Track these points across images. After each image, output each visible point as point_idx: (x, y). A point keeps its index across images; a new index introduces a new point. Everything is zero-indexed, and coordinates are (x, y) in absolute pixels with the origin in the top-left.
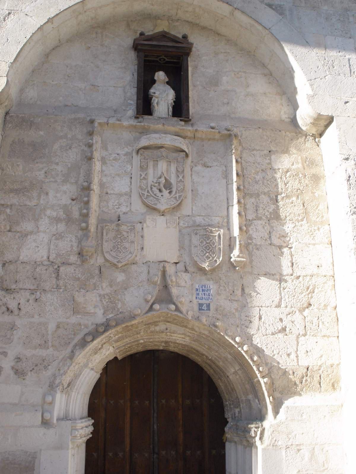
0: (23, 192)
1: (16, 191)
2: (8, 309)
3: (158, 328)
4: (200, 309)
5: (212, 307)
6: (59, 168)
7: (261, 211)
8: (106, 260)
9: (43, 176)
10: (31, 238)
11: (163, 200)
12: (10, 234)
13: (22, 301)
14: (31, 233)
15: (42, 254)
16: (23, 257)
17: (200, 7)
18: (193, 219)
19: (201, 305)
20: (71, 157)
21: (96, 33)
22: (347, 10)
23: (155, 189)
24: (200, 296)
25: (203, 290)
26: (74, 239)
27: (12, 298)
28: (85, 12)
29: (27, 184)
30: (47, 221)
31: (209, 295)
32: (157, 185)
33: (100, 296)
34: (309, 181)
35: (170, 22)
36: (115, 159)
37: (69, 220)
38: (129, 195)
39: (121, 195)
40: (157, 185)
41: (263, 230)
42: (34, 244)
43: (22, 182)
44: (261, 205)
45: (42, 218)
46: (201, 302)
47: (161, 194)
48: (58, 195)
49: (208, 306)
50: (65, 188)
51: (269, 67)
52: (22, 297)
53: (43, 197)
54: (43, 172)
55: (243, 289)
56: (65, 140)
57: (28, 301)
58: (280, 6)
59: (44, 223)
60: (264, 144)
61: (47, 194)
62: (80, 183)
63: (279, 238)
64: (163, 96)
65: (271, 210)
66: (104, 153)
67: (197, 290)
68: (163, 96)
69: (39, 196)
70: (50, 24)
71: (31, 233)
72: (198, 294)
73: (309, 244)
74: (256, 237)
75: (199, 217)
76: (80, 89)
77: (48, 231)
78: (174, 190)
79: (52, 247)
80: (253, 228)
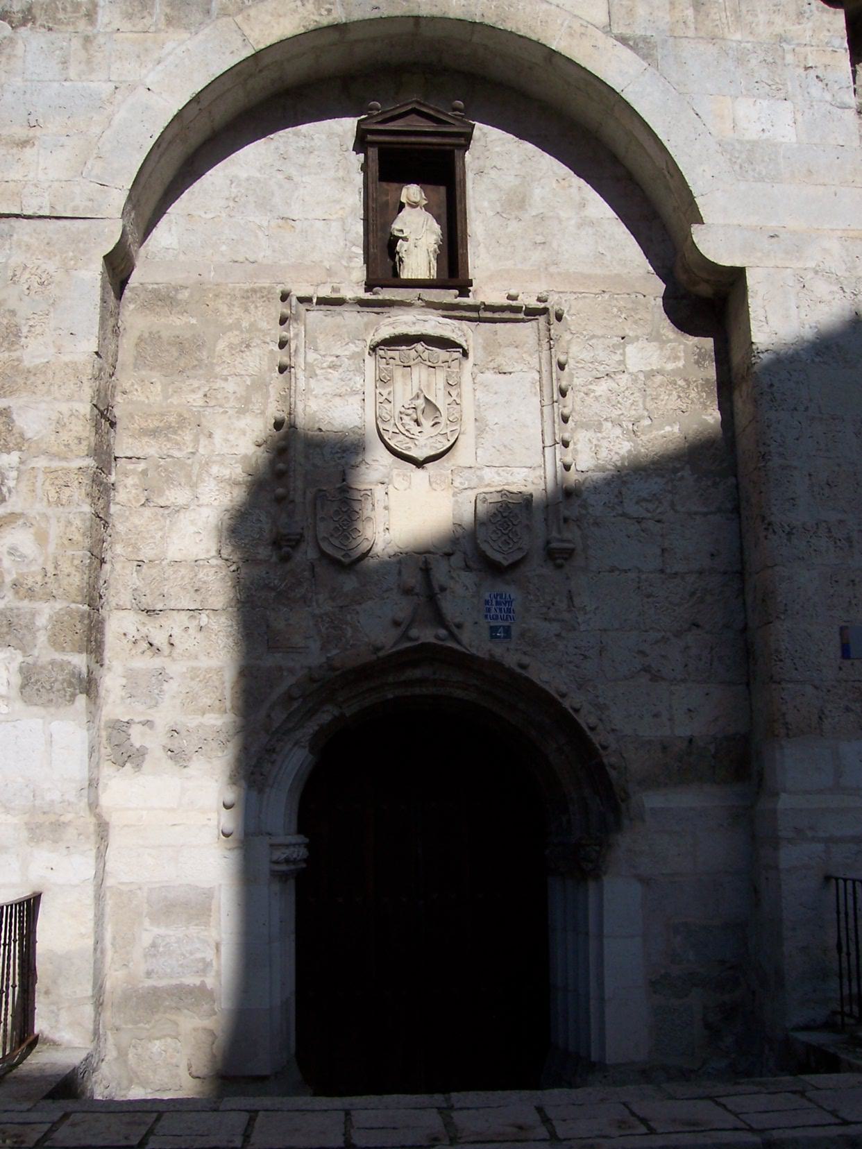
0: (166, 435)
1: (153, 433)
4: (492, 637)
5: (515, 632)
6: (231, 386)
8: (323, 554)
9: (201, 403)
10: (184, 519)
11: (421, 440)
12: (147, 512)
13: (177, 632)
14: (185, 508)
16: (173, 553)
18: (478, 473)
19: (493, 629)
20: (251, 364)
22: (781, 39)
23: (406, 419)
24: (493, 612)
25: (497, 603)
26: (263, 518)
28: (260, 71)
29: (172, 419)
31: (509, 610)
32: (410, 412)
36: (333, 367)
43: (163, 415)
44: (604, 443)
45: (204, 481)
46: (493, 623)
47: (419, 429)
49: (507, 630)
53: (203, 441)
54: (201, 394)
55: (571, 598)
56: (237, 333)
58: (645, 39)
60: (612, 323)
61: (210, 435)
63: (637, 503)
64: (419, 238)
66: (312, 356)
67: (487, 602)
68: (419, 238)
69: (196, 441)
70: (194, 105)
71: (185, 508)
72: (489, 610)
75: (487, 469)
76: (260, 227)
78: (443, 420)
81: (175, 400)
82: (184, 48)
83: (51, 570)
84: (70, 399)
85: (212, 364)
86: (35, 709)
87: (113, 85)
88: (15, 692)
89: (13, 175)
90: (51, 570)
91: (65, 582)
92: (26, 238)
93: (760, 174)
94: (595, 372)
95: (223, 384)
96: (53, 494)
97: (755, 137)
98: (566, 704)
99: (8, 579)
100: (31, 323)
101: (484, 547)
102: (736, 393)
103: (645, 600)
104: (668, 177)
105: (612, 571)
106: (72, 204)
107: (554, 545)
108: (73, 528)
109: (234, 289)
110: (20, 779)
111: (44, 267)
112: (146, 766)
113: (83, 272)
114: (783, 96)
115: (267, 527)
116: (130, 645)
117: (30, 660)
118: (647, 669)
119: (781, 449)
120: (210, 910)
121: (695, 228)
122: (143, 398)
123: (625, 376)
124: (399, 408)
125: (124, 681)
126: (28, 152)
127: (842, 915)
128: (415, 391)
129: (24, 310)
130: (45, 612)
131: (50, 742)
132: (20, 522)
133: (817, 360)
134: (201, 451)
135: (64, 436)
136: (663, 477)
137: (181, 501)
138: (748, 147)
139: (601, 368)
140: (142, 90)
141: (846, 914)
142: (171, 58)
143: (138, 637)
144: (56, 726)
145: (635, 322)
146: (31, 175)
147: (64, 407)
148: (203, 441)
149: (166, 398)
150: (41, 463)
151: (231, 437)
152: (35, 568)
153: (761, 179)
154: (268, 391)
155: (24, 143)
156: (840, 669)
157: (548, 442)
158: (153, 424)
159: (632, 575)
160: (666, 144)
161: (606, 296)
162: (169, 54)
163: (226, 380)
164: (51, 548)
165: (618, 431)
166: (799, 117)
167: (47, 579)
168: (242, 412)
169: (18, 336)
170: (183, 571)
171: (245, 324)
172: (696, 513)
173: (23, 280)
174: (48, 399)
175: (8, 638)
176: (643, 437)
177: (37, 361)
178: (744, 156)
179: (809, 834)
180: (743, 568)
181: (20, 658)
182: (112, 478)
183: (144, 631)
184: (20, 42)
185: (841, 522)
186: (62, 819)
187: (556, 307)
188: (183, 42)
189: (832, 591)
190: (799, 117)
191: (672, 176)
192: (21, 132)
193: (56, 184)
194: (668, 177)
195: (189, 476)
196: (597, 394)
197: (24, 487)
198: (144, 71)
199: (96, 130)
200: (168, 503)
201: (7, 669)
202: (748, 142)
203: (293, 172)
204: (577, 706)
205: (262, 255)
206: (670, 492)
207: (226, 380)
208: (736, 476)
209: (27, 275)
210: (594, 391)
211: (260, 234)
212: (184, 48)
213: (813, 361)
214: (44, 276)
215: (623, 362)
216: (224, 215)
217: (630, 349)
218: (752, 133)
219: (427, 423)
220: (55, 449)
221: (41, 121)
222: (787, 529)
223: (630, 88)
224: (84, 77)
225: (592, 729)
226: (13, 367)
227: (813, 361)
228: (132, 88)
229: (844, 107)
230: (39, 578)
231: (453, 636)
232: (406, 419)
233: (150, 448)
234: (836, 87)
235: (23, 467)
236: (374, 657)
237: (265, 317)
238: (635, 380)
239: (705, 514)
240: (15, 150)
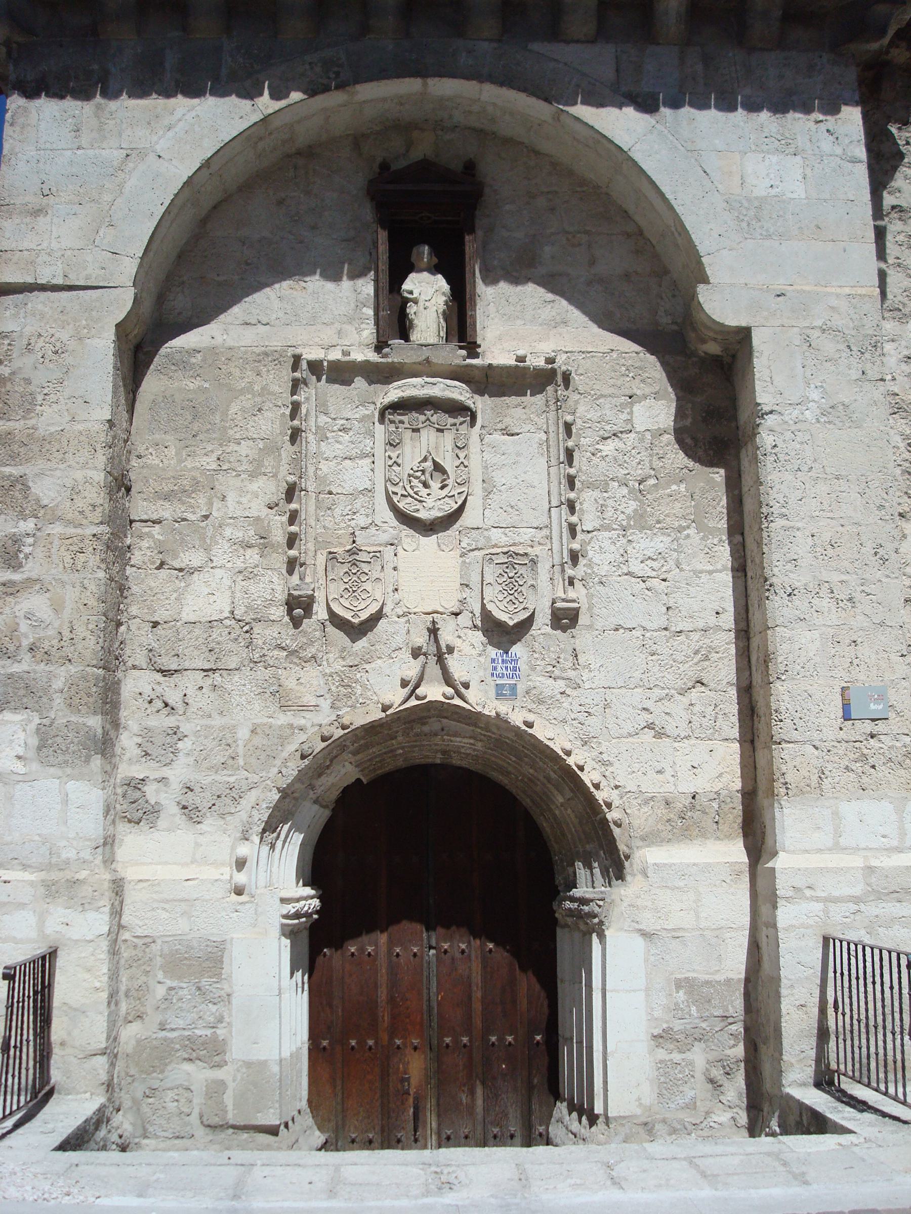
1: (167, 497)
2: (166, 705)
3: (426, 729)
4: (498, 695)
5: (521, 689)
6: (244, 449)
7: (610, 514)
8: (332, 614)
11: (430, 502)
12: (163, 573)
14: (199, 569)
15: (220, 606)
16: (187, 615)
17: (494, 104)
18: (486, 533)
20: (263, 427)
21: (295, 168)
25: (503, 661)
26: (275, 579)
27: (173, 686)
28: (270, 134)
30: (226, 545)
31: (515, 669)
32: (419, 474)
33: (325, 675)
34: (705, 451)
35: (440, 133)
36: (344, 430)
37: (264, 542)
38: (368, 491)
39: (353, 495)
41: (613, 548)
42: (207, 590)
44: (610, 502)
45: (217, 543)
46: (499, 682)
48: (244, 500)
49: (513, 688)
50: (255, 486)
51: (637, 218)
52: (190, 682)
53: (217, 504)
54: (214, 457)
56: (250, 396)
57: (201, 688)
59: (221, 552)
62: (280, 476)
65: (629, 511)
66: (323, 419)
67: (493, 661)
70: (204, 170)
71: (199, 569)
72: (495, 668)
73: (701, 572)
74: (601, 563)
77: (229, 565)
78: (450, 482)
79: (238, 595)
81: (189, 464)
82: (193, 114)
83: (66, 634)
84: (85, 466)
85: (225, 428)
86: (52, 770)
87: (124, 152)
88: (31, 754)
89: (26, 245)
90: (66, 634)
91: (80, 647)
92: (40, 307)
93: (767, 231)
94: (601, 433)
95: (236, 448)
96: (68, 559)
97: (764, 194)
98: (571, 761)
99: (25, 643)
100: (46, 391)
101: (490, 607)
102: (743, 452)
103: (650, 658)
104: (676, 234)
105: (617, 630)
106: (86, 272)
107: (559, 605)
108: (88, 594)
109: (246, 352)
110: (37, 838)
111: (57, 335)
112: (162, 823)
113: (97, 340)
114: (792, 150)
115: (279, 588)
116: (147, 705)
117: (46, 722)
118: (650, 726)
119: (784, 510)
120: (222, 962)
121: (701, 288)
122: (157, 462)
123: (632, 435)
125: (139, 740)
126: (42, 220)
127: (838, 975)
128: (424, 453)
129: (39, 378)
130: (61, 676)
131: (66, 801)
132: (37, 587)
133: (822, 420)
134: (215, 514)
135: (80, 503)
136: (669, 535)
137: (196, 563)
138: (756, 204)
139: (608, 428)
140: (152, 157)
141: (842, 974)
142: (181, 124)
143: (153, 697)
144: (71, 785)
145: (643, 381)
146: (45, 245)
147: (79, 475)
148: (217, 504)
149: (181, 461)
150: (57, 529)
151: (244, 500)
152: (51, 632)
153: (769, 237)
154: (280, 455)
155: (37, 212)
156: (841, 729)
157: (555, 503)
158: (167, 487)
159: (638, 633)
160: (673, 202)
161: (614, 355)
162: (180, 120)
163: (239, 444)
164: (66, 614)
165: (625, 491)
166: (808, 171)
167: (62, 643)
169: (33, 403)
170: (197, 632)
172: (701, 572)
173: (37, 348)
174: (61, 466)
175: (25, 700)
176: (648, 496)
177: (52, 429)
178: (752, 213)
179: (808, 893)
180: (748, 626)
181: (37, 721)
182: (128, 541)
183: (159, 689)
184: (34, 112)
185: (842, 582)
186: (77, 876)
187: (564, 368)
188: (193, 108)
189: (833, 652)
190: (808, 171)
191: (680, 234)
192: (34, 200)
193: (69, 253)
194: (676, 234)
195: (203, 539)
196: (604, 454)
197: (40, 552)
198: (155, 138)
199: (107, 197)
200: (183, 566)
201: (24, 730)
202: (756, 198)
204: (581, 763)
205: (274, 316)
206: (675, 550)
207: (239, 444)
208: (742, 534)
209: (41, 343)
212: (193, 114)
213: (818, 421)
214: (58, 344)
215: (629, 421)
217: (636, 408)
218: (761, 190)
219: (435, 485)
220: (70, 516)
221: (54, 189)
222: (789, 590)
223: (638, 146)
224: (96, 145)
225: (597, 786)
226: (28, 435)
227: (818, 421)
228: (142, 154)
229: (854, 161)
230: (55, 642)
232: (415, 482)
233: (166, 511)
234: (847, 141)
235: (38, 534)
236: (383, 715)
237: (278, 381)
238: (642, 440)
239: (710, 572)
240: (28, 220)
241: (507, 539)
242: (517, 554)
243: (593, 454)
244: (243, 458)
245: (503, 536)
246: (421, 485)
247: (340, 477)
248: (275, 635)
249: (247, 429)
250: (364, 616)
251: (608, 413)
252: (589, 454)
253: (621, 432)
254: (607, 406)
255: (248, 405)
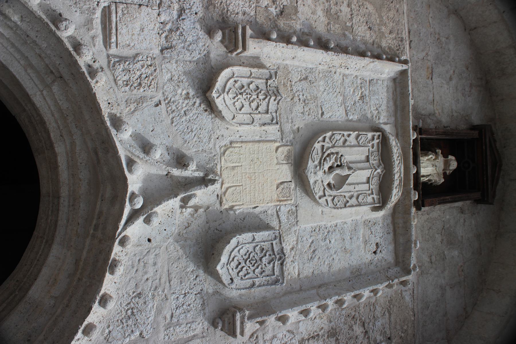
20: (360, 29)
40: (339, 163)
50: (320, 13)
56: (378, 22)
75: (295, 239)
78: (334, 193)
80: (287, 337)
94: (368, 321)
107: (238, 316)
124: (342, 151)
139: (371, 326)
168: (327, 12)
171: (383, 29)
196: (354, 327)
203: (454, 82)
205: (415, 53)
210: (355, 323)
211: (424, 54)
216: (432, 30)
219: (330, 179)
231: (134, 215)
232: (333, 158)
241: (289, 251)
242: (282, 264)
243: (353, 318)
244: (339, 6)
245: (291, 247)
246: (330, 164)
247: (331, 90)
248: (194, 9)
249: (357, 15)
250: (219, 102)
251: (379, 324)
252: (353, 314)
253: (368, 338)
254: (384, 321)
255: (373, 19)
